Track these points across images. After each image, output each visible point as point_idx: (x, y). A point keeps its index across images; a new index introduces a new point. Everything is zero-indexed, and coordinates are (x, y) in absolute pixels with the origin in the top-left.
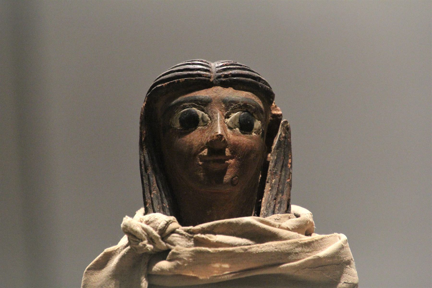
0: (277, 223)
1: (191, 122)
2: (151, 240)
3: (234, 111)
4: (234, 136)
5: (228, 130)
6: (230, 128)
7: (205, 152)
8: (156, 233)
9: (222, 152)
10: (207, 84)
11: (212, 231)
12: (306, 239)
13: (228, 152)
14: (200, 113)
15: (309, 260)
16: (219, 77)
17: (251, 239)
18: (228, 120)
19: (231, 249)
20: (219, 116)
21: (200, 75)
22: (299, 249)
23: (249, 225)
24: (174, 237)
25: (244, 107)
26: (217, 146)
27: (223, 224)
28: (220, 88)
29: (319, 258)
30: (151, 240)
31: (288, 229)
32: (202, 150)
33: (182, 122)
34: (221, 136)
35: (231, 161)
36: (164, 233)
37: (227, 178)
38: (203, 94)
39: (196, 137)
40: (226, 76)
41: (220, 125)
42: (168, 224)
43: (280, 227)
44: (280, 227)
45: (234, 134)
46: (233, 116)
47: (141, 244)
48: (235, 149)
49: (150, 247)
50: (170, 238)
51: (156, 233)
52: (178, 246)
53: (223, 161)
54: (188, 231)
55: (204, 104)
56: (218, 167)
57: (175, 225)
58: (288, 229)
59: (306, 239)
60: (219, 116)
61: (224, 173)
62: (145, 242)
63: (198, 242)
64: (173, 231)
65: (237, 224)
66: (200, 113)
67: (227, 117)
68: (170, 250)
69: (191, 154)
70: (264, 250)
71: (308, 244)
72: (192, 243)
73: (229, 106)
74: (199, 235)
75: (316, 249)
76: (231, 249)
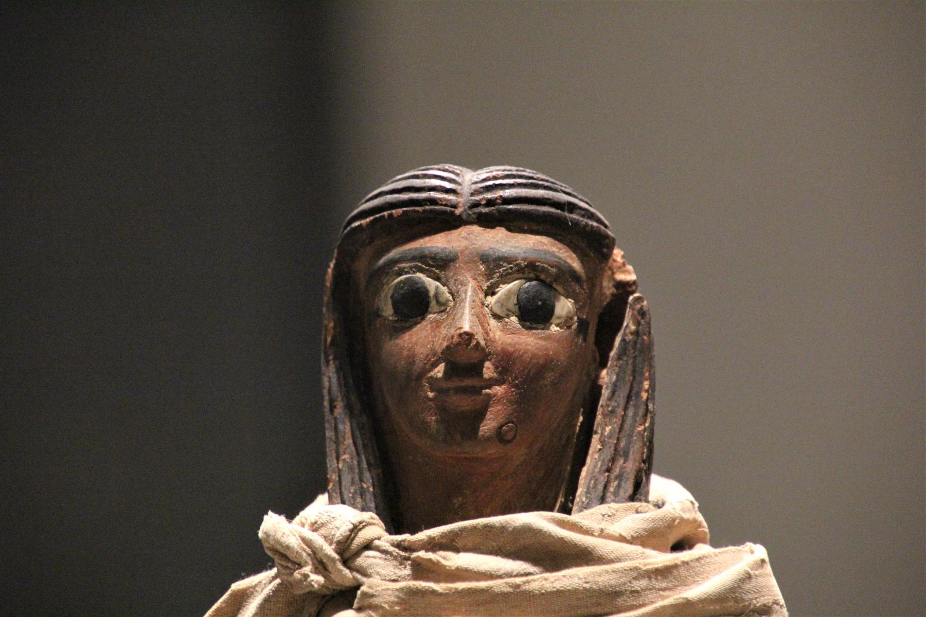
0: (596, 526)
1: (415, 305)
2: (321, 565)
3: (506, 278)
4: (509, 335)
5: (493, 322)
6: (496, 316)
7: (439, 371)
8: (329, 550)
9: (475, 369)
10: (448, 221)
11: (450, 544)
12: (660, 559)
13: (489, 370)
14: (431, 284)
15: (664, 608)
16: (476, 205)
17: (535, 561)
18: (491, 300)
19: (483, 584)
20: (470, 290)
21: (433, 201)
22: (643, 583)
23: (527, 530)
24: (368, 559)
25: (530, 269)
26: (464, 360)
27: (475, 528)
28: (476, 229)
29: (688, 603)
30: (321, 565)
31: (622, 539)
32: (435, 365)
33: (395, 305)
34: (470, 336)
35: (499, 390)
36: (348, 551)
37: (488, 426)
38: (438, 243)
39: (423, 339)
40: (490, 203)
41: (473, 312)
42: (356, 529)
43: (602, 534)
44: (602, 534)
45: (505, 329)
46: (503, 289)
47: (297, 575)
48: (507, 363)
49: (317, 580)
50: (361, 561)
51: (329, 550)
52: (375, 580)
53: (477, 391)
54: (398, 545)
55: (440, 264)
56: (464, 403)
57: (376, 530)
58: (622, 539)
59: (660, 559)
60: (470, 290)
61: (480, 415)
62: (307, 569)
63: (421, 570)
64: (368, 546)
65: (503, 528)
66: (431, 284)
67: (490, 292)
68: (358, 586)
69: (414, 377)
70: (558, 585)
71: (664, 572)
72: (407, 571)
73: (495, 268)
74: (422, 554)
75: (684, 583)
76: (483, 584)
